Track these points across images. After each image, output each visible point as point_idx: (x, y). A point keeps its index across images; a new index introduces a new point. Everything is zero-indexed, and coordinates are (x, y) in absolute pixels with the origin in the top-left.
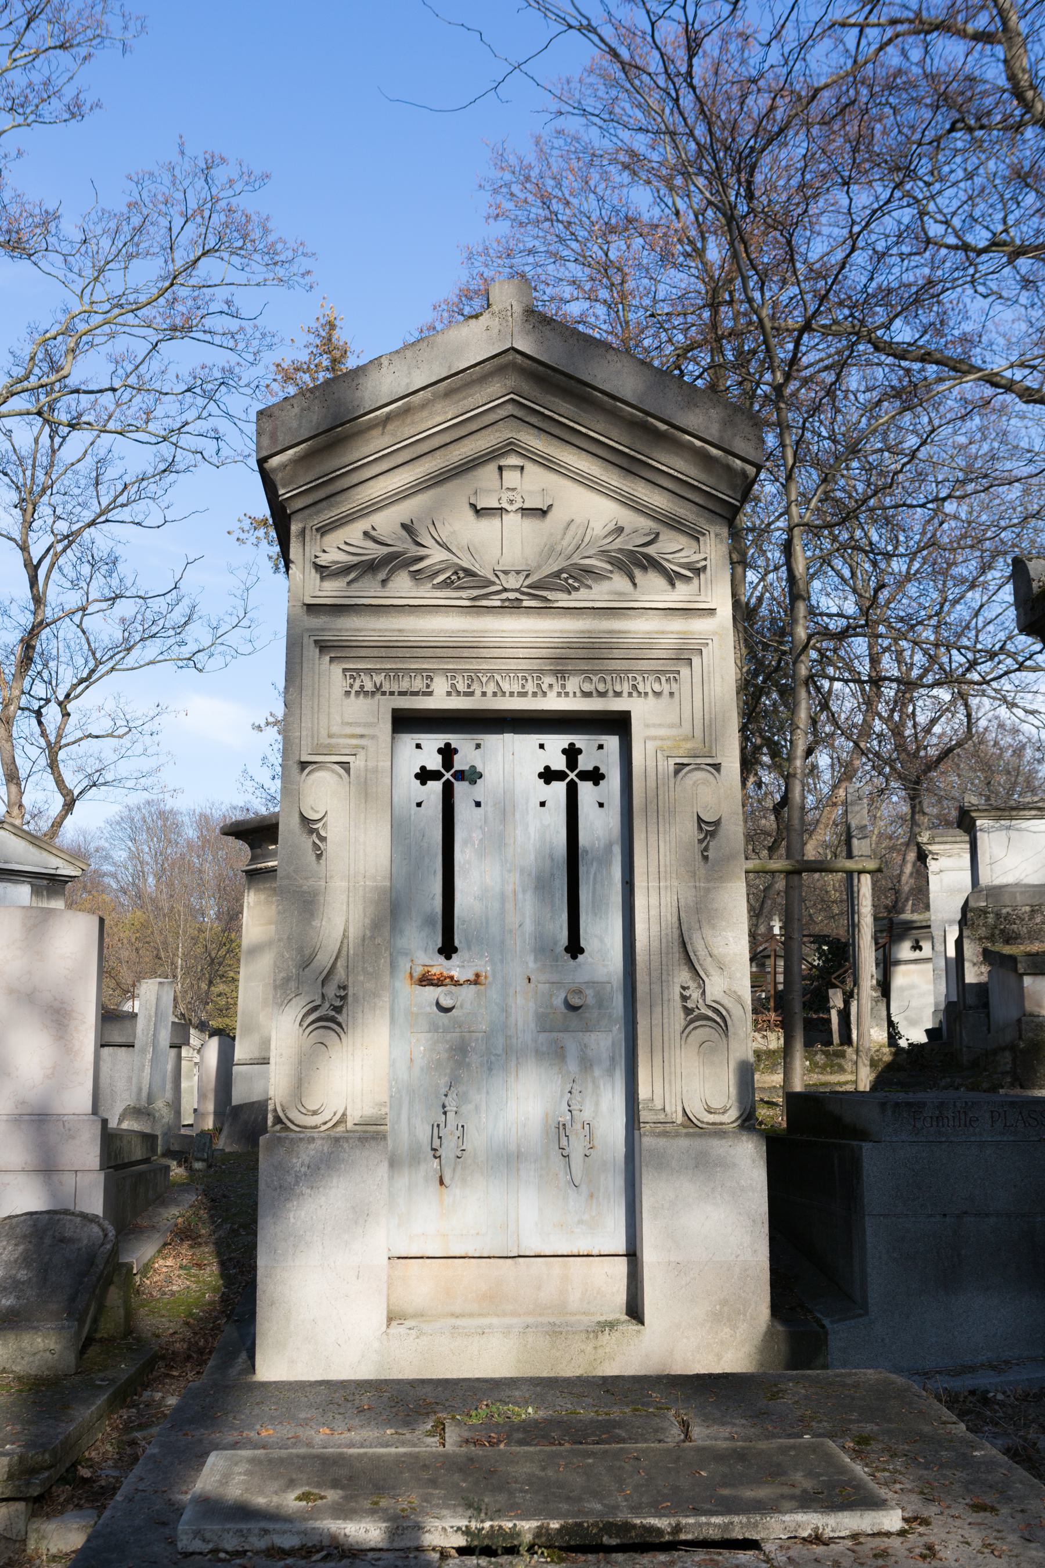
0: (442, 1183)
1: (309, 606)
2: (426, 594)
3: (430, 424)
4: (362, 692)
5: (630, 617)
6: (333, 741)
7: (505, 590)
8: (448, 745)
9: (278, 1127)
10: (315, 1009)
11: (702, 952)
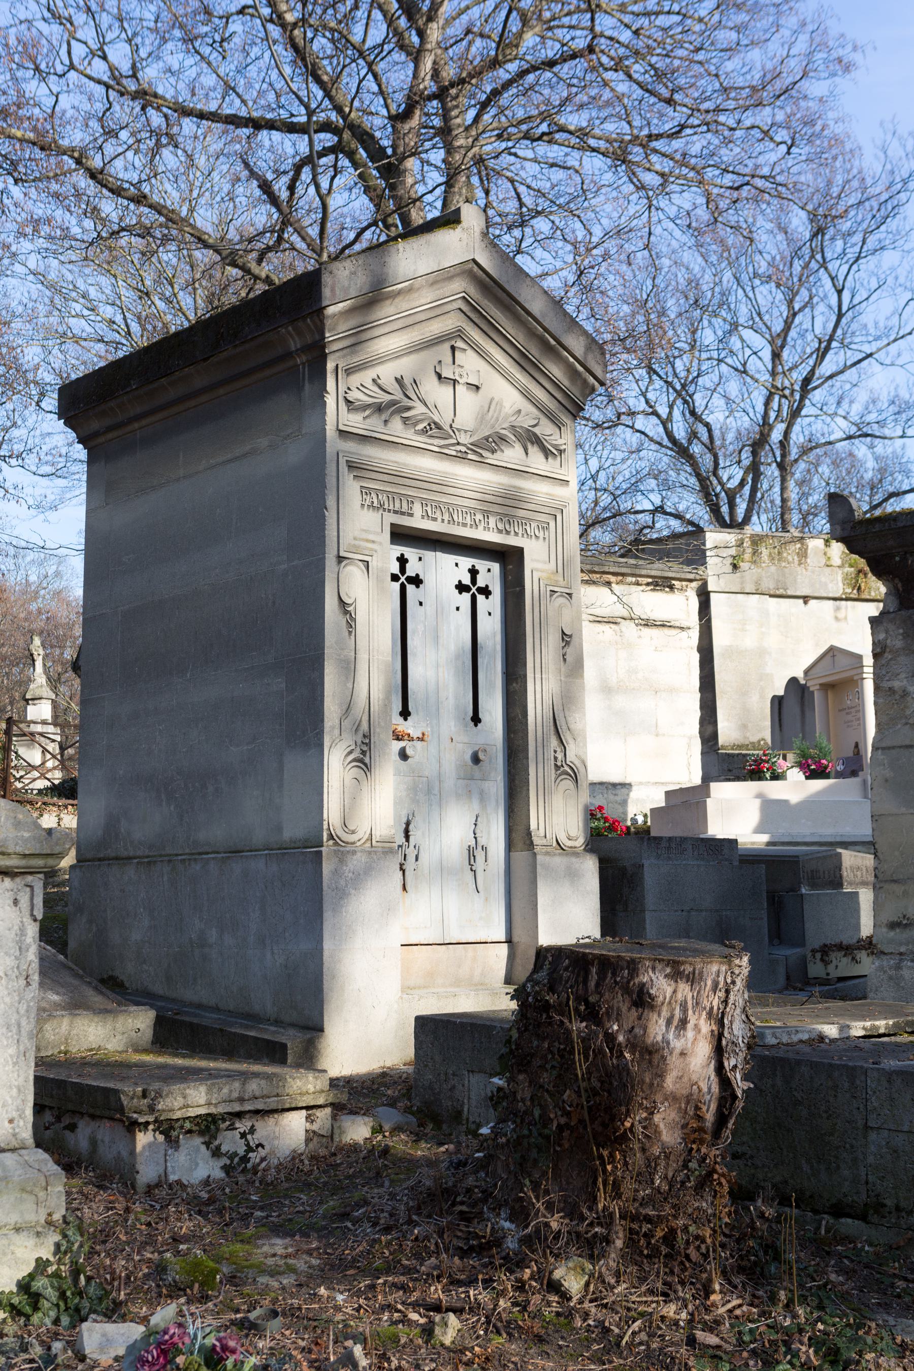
0: (404, 888)
1: (341, 431)
2: (410, 436)
3: (417, 304)
4: (371, 506)
5: (525, 478)
6: (357, 543)
7: (458, 444)
8: (402, 555)
9: (331, 842)
10: (350, 752)
11: (564, 727)
